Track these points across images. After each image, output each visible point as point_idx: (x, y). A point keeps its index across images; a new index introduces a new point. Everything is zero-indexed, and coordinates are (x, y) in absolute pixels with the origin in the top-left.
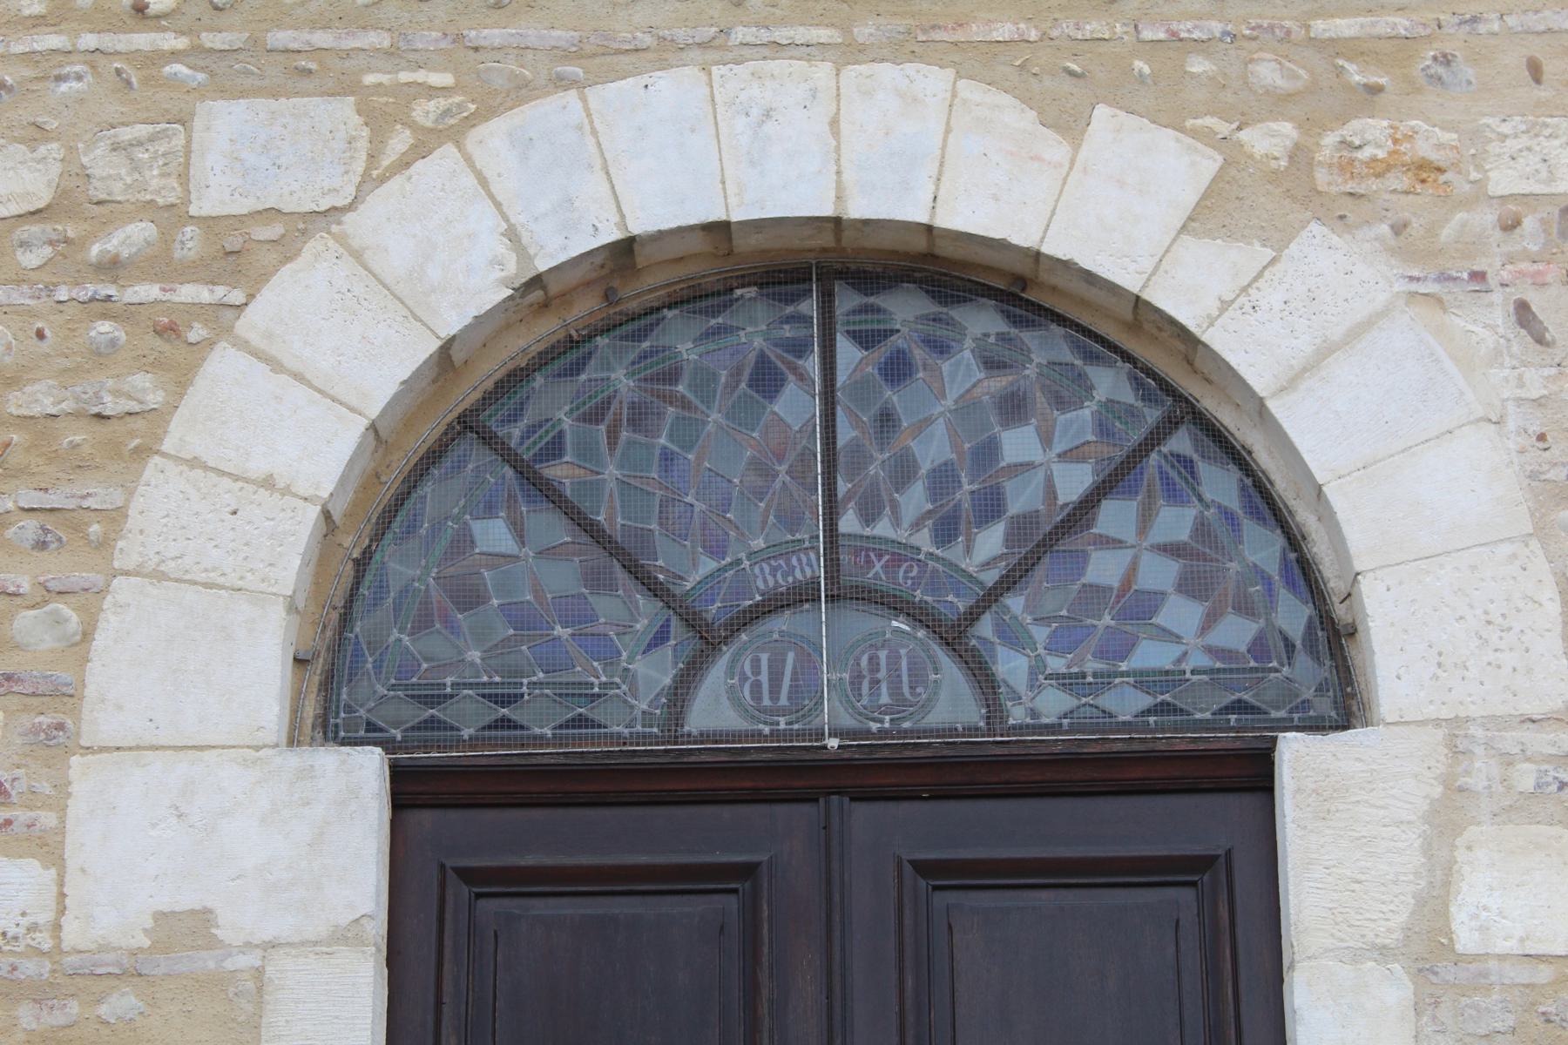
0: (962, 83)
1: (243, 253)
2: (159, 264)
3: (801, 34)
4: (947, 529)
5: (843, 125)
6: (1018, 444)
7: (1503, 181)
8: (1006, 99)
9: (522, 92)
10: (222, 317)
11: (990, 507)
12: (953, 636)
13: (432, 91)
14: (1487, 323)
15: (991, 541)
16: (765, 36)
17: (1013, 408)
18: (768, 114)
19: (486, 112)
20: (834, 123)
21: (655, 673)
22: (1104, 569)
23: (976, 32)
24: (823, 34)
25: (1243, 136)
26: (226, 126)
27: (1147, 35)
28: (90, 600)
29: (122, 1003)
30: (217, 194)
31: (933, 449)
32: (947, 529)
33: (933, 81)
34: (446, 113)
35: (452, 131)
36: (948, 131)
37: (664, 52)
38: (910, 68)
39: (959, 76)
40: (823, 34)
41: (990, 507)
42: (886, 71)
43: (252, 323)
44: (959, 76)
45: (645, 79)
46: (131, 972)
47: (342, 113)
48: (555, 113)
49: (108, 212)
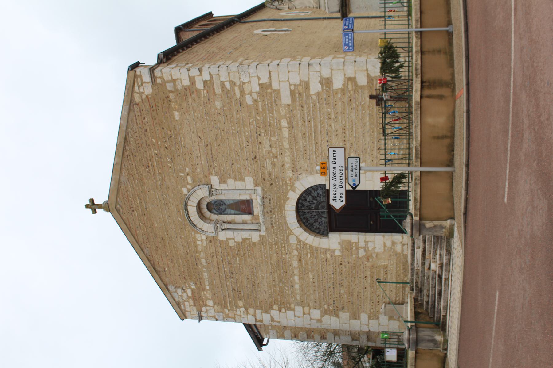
1: (299, 241)
2: (300, 245)
4: (314, 203)
6: (308, 200)
7: (291, 175)
9: (288, 227)
10: (303, 242)
11: (312, 201)
12: (320, 203)
14: (300, 177)
15: (314, 201)
17: (306, 200)
21: (323, 219)
22: (316, 195)
26: (291, 242)
28: (321, 248)
29: (344, 246)
30: (296, 242)
31: (309, 204)
32: (314, 203)
33: (286, 206)
35: (291, 231)
37: (285, 220)
41: (312, 201)
43: (303, 240)
46: (342, 246)
47: (290, 236)
48: (289, 225)
49: (297, 247)
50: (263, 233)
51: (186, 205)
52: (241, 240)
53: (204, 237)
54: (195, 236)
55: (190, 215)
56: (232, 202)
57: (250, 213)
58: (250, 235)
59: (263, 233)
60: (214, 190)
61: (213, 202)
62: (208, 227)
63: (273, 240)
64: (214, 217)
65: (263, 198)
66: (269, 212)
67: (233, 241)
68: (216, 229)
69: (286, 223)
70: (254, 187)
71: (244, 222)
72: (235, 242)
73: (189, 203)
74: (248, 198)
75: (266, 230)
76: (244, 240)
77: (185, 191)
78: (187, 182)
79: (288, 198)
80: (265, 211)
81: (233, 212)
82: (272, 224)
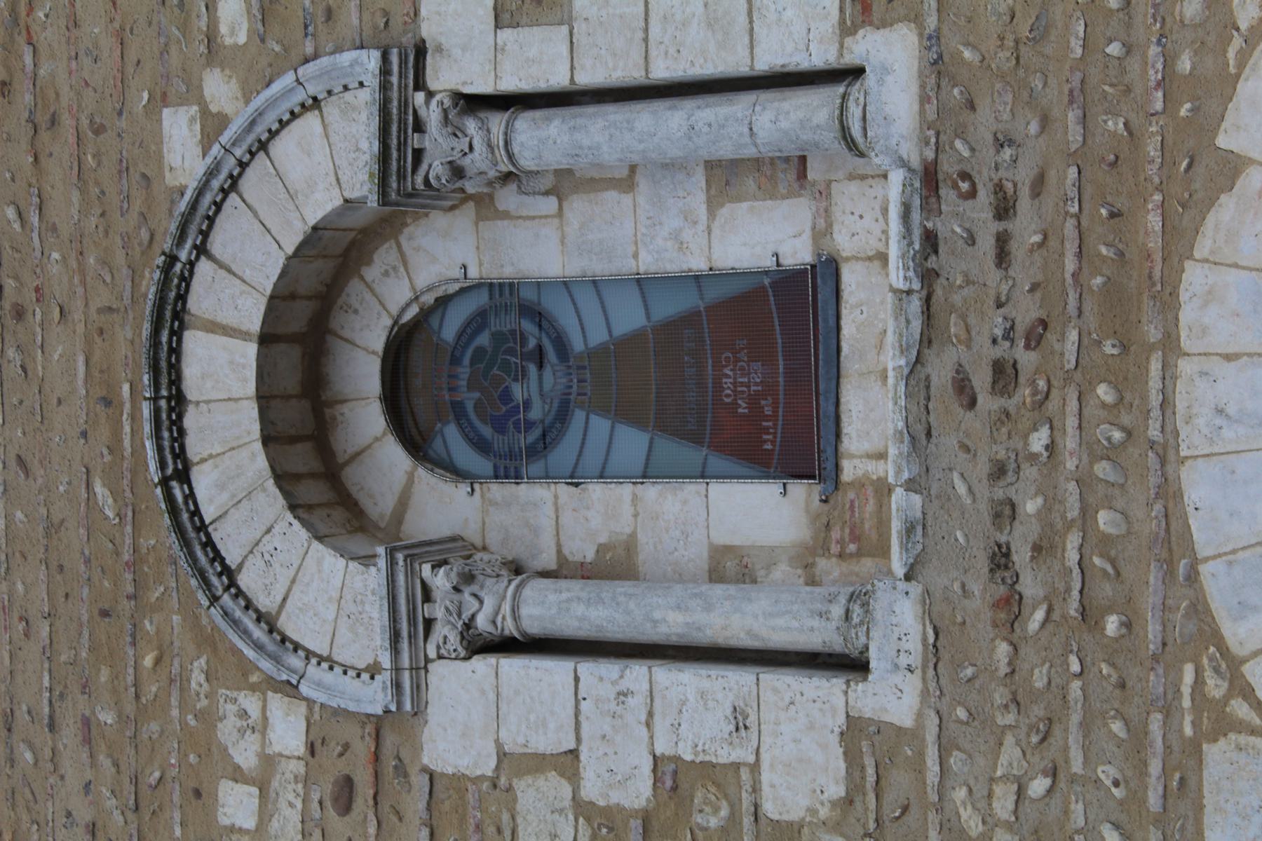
0: (1197, 255)
3: (1154, 383)
5: (1230, 350)
8: (1211, 219)
13: (1199, 681)
16: (1156, 413)
18: (1220, 411)
19: (1217, 638)
20: (1229, 357)
23: (1155, 244)
24: (1155, 366)
25: (1243, 26)
27: (1159, 106)
33: (1194, 278)
34: (1216, 670)
35: (1232, 666)
36: (1236, 266)
37: (1169, 494)
38: (1184, 296)
39: (1190, 257)
40: (1155, 366)
42: (1187, 315)
44: (1190, 257)
45: (1190, 510)
47: (1217, 755)
48: (1217, 583)
50: (892, 696)
51: (171, 316)
52: (638, 792)
53: (288, 731)
54: (209, 719)
55: (194, 447)
56: (629, 317)
57: (794, 443)
58: (740, 722)
59: (892, 696)
60: (432, 116)
61: (450, 326)
62: (325, 594)
63: (1003, 805)
64: (443, 506)
65: (929, 179)
66: (981, 380)
67: (555, 787)
68: (408, 624)
69: (1173, 545)
70: (846, 30)
71: (731, 567)
72: (582, 808)
73: (209, 294)
74: (798, 253)
75: (934, 652)
76: (674, 777)
77: (183, 153)
78: (211, 37)
79: (1232, 168)
80: (940, 371)
81: (632, 443)
82: (1001, 559)
